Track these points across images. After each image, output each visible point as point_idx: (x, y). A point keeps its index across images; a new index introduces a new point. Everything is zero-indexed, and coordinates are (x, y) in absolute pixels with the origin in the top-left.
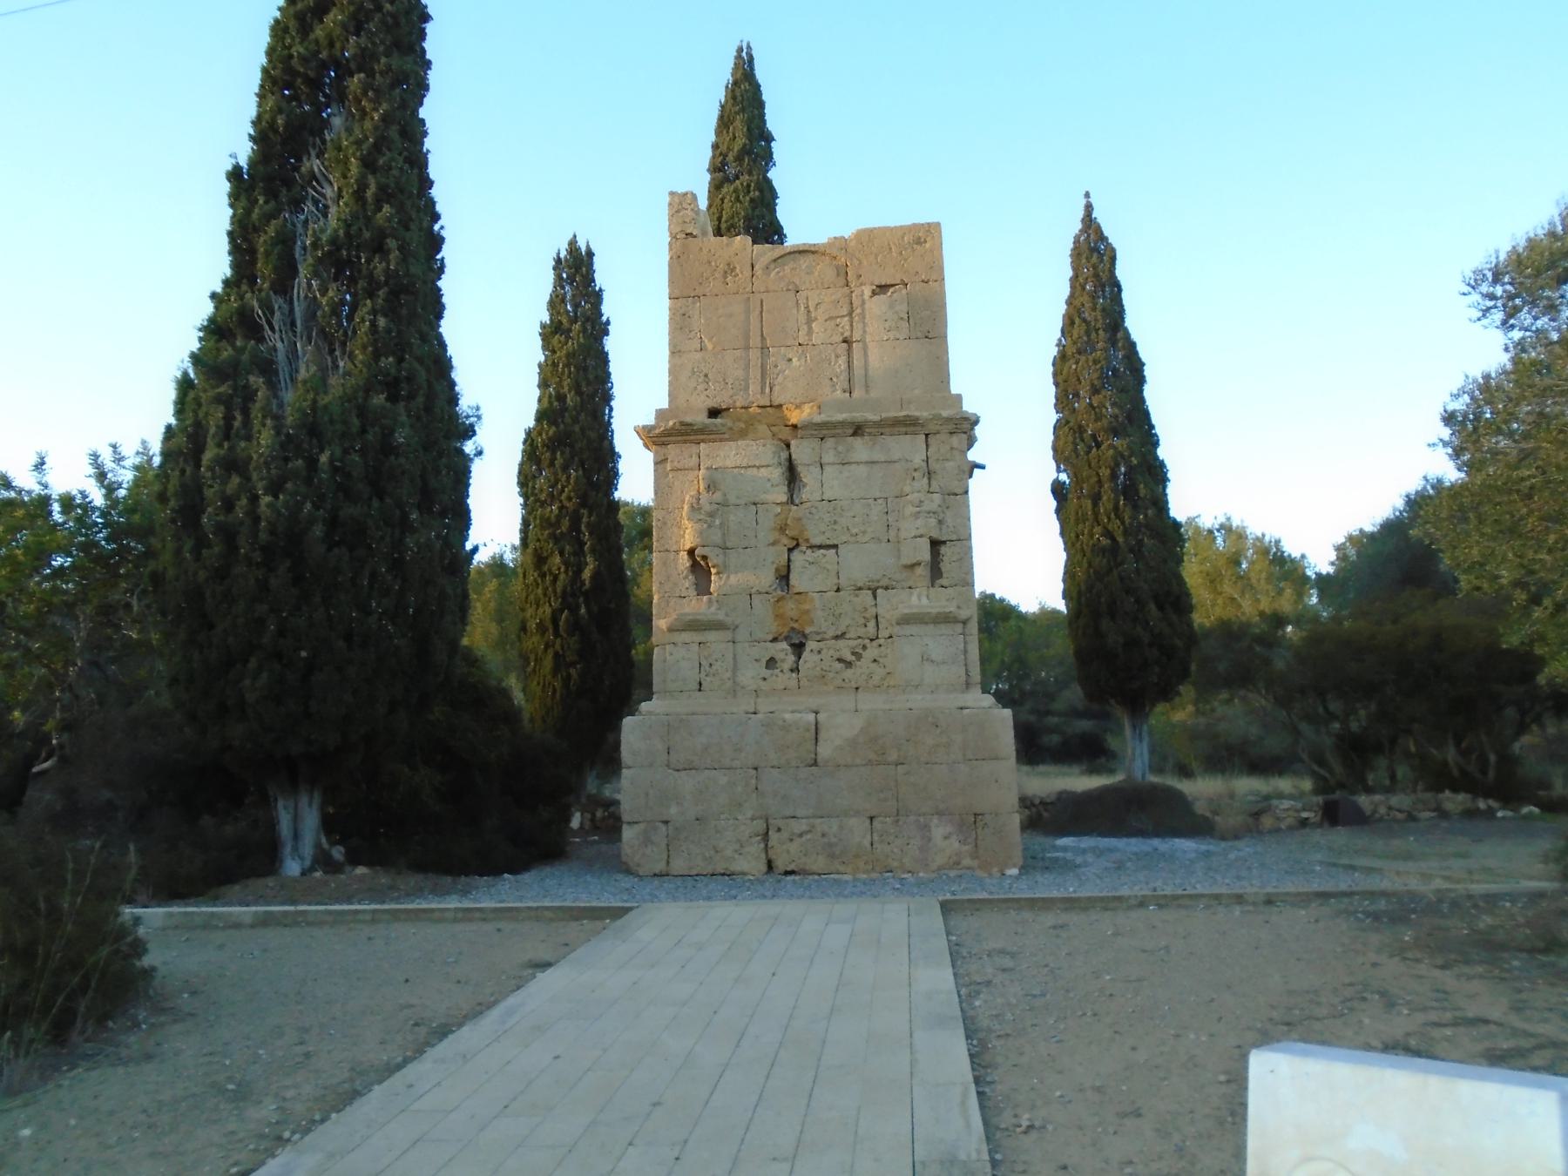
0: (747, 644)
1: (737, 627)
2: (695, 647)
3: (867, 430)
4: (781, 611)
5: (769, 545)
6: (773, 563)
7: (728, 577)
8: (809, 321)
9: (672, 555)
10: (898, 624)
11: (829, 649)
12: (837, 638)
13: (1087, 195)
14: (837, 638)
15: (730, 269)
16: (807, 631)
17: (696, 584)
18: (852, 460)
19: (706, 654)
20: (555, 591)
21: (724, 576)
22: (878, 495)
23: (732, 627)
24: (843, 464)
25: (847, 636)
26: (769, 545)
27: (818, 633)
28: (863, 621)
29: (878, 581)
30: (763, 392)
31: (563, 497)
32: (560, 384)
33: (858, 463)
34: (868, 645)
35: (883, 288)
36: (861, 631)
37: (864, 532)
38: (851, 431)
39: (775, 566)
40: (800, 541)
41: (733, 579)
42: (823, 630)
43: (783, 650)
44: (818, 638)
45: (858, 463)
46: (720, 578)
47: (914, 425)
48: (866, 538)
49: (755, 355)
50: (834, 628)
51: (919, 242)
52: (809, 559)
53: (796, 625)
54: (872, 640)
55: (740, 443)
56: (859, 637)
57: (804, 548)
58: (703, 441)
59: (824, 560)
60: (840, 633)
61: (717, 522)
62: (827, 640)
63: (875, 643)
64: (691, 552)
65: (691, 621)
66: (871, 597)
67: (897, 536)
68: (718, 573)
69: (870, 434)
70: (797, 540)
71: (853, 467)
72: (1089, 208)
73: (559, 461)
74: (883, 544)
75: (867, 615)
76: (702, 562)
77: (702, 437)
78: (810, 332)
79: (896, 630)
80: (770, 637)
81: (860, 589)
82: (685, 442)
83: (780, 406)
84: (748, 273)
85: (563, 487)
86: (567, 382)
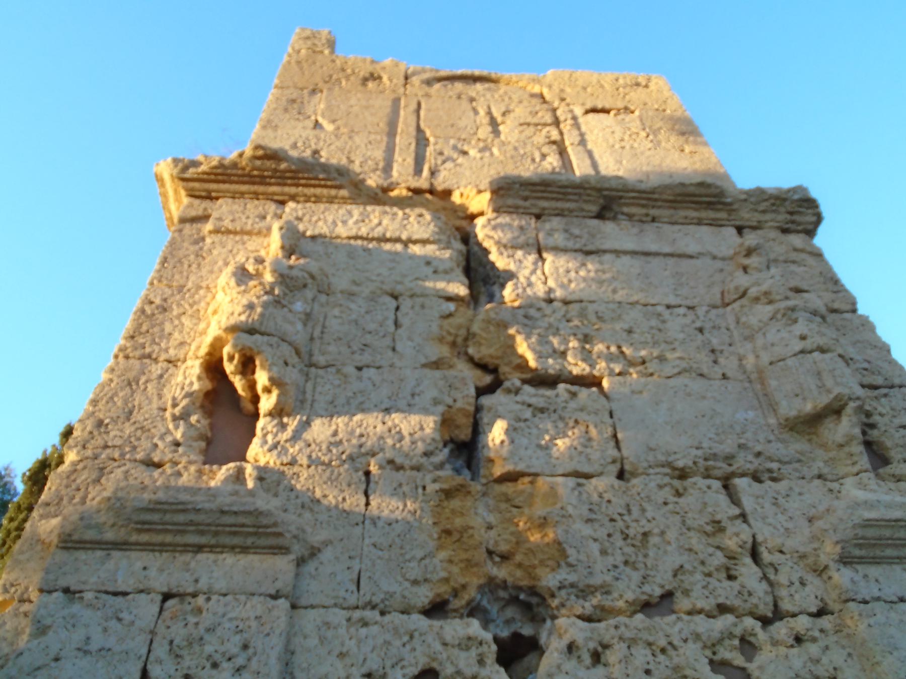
0: (338, 616)
1: (314, 552)
2: (147, 607)
3: (626, 210)
4: (458, 522)
5: (424, 366)
6: (436, 402)
7: (306, 424)
9: (156, 369)
10: (845, 560)
11: (631, 643)
12: (646, 607)
14: (646, 607)
16: (549, 580)
17: (209, 442)
18: (607, 246)
19: (178, 632)
21: (293, 423)
22: (672, 300)
23: (297, 549)
24: (588, 253)
25: (683, 603)
26: (424, 366)
27: (584, 592)
28: (719, 559)
29: (729, 458)
30: (418, 171)
33: (617, 253)
34: (761, 636)
36: (726, 592)
37: (661, 359)
38: (594, 208)
39: (441, 409)
40: (503, 369)
41: (320, 430)
42: (597, 580)
43: (468, 643)
44: (587, 606)
45: (617, 253)
46: (283, 427)
47: (710, 205)
48: (668, 370)
50: (636, 576)
52: (533, 401)
53: (501, 572)
54: (766, 622)
55: (369, 208)
56: (723, 609)
57: (518, 383)
58: (293, 198)
59: (573, 405)
60: (658, 592)
61: (299, 306)
62: (619, 612)
63: (781, 629)
65: (156, 507)
66: (722, 498)
67: (741, 366)
68: (278, 413)
69: (630, 217)
70: (494, 371)
71: (607, 257)
74: (718, 383)
75: (731, 543)
76: (238, 383)
77: (293, 190)
79: (843, 577)
80: (424, 596)
81: (683, 474)
82: (256, 196)
83: (448, 193)
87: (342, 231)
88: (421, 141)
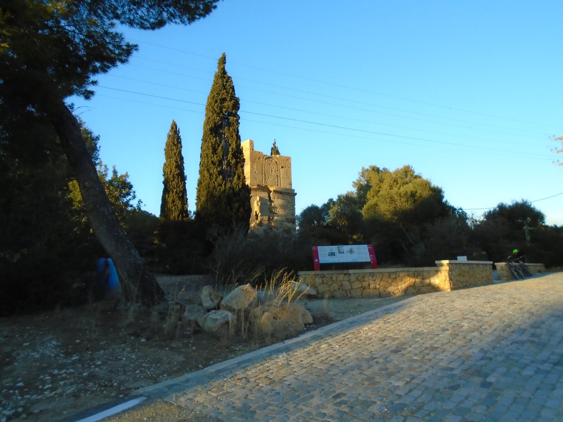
8: (272, 171)
13: (275, 140)
15: (259, 158)
20: (178, 210)
31: (180, 187)
32: (177, 159)
35: (282, 167)
49: (263, 175)
51: (288, 160)
64: (256, 212)
72: (275, 143)
73: (179, 179)
78: (272, 173)
84: (262, 159)
85: (180, 185)
86: (178, 159)
87: (261, 196)
88: (265, 174)
